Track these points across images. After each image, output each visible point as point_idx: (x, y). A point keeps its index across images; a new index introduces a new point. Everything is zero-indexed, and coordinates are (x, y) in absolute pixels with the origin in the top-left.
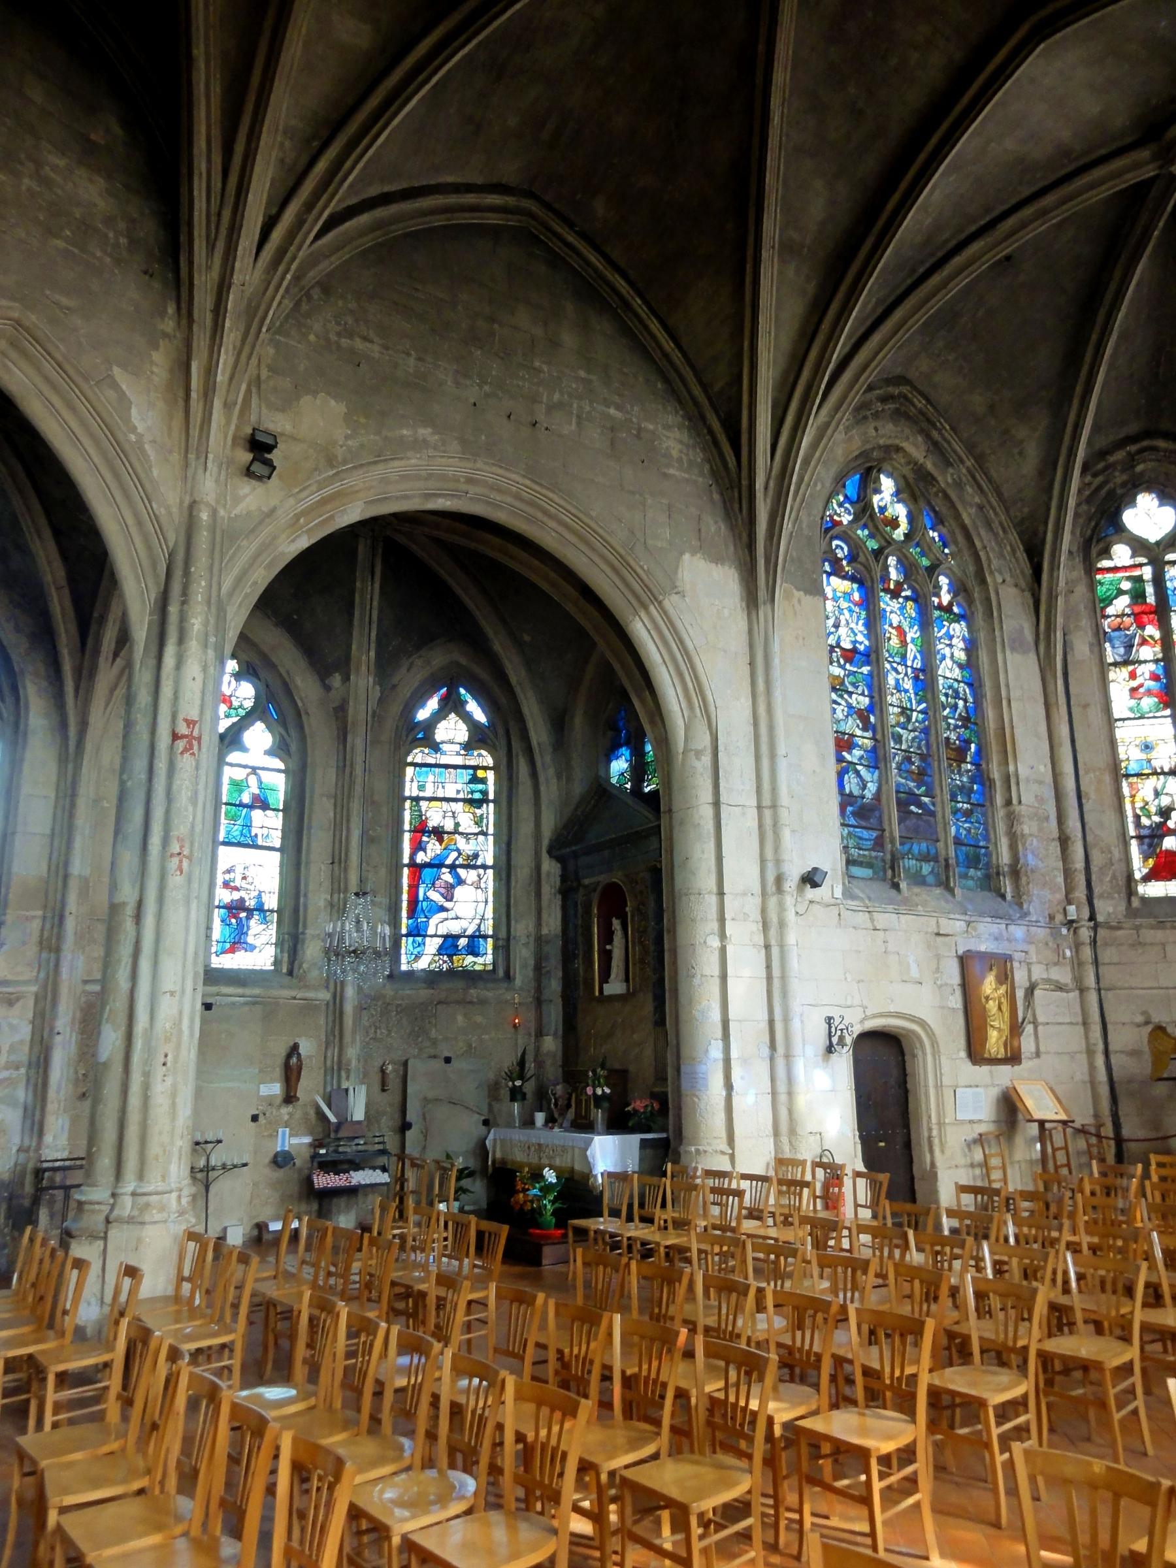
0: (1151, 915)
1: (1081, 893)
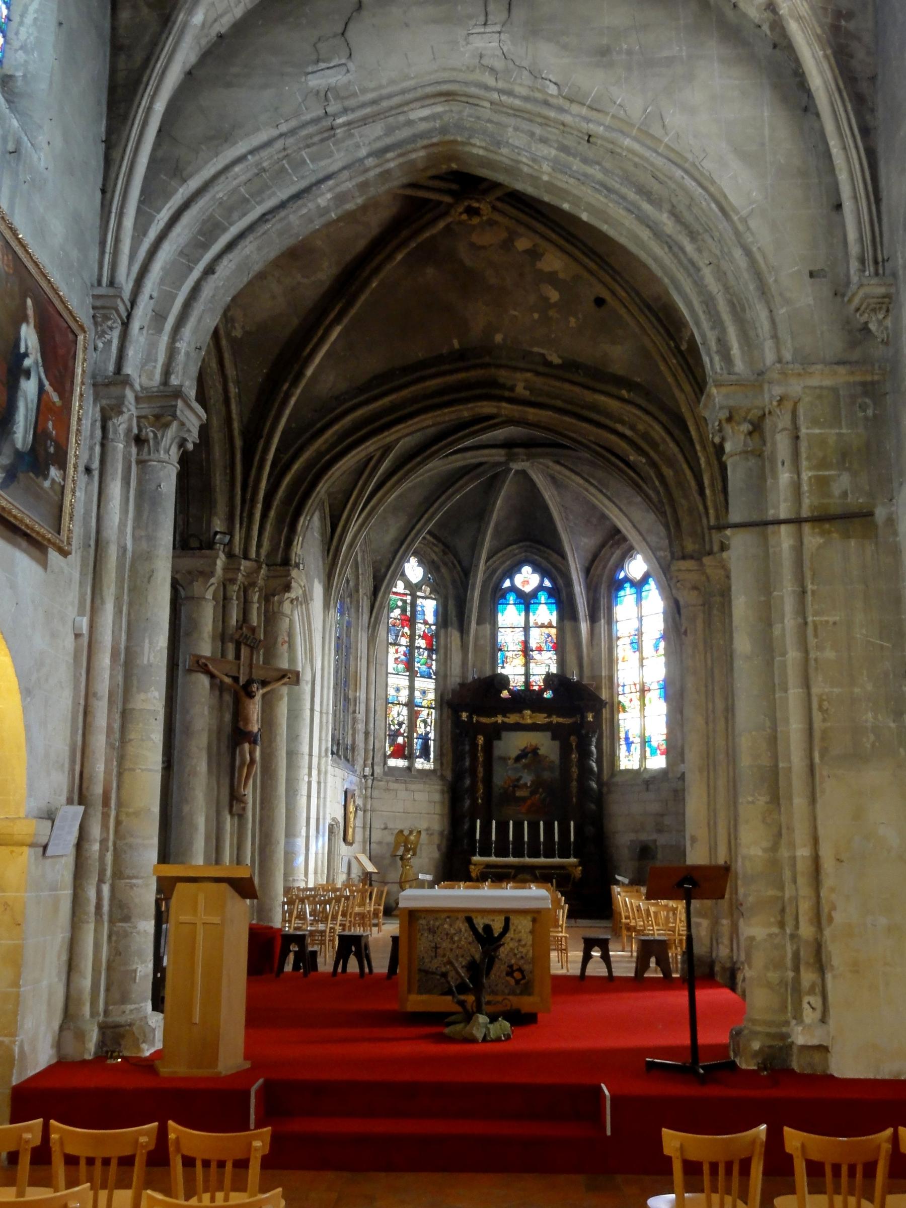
0: (393, 775)
1: (370, 762)
